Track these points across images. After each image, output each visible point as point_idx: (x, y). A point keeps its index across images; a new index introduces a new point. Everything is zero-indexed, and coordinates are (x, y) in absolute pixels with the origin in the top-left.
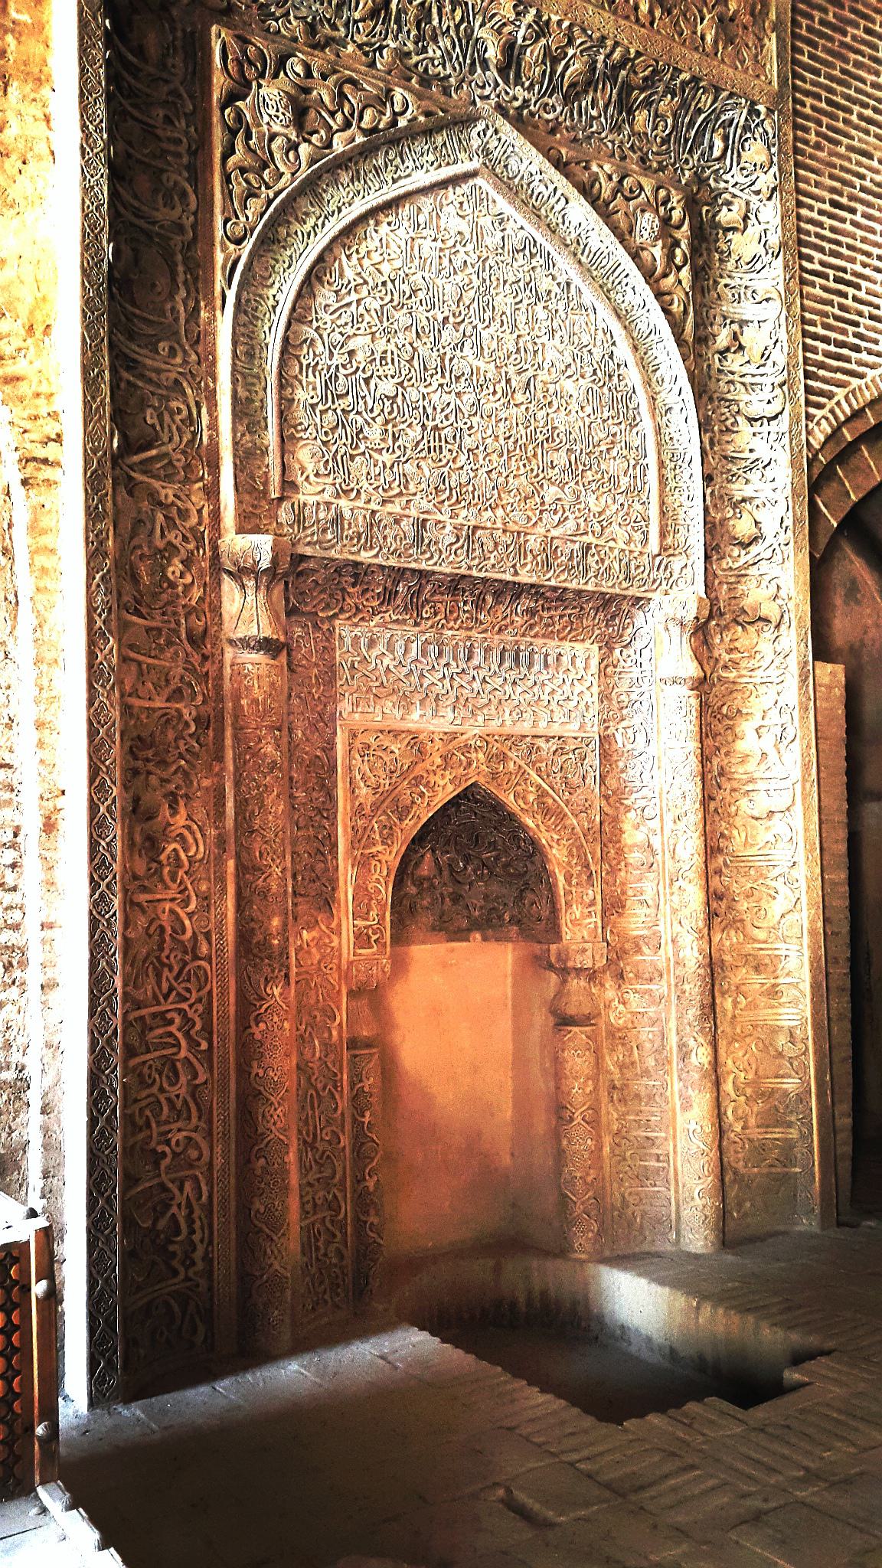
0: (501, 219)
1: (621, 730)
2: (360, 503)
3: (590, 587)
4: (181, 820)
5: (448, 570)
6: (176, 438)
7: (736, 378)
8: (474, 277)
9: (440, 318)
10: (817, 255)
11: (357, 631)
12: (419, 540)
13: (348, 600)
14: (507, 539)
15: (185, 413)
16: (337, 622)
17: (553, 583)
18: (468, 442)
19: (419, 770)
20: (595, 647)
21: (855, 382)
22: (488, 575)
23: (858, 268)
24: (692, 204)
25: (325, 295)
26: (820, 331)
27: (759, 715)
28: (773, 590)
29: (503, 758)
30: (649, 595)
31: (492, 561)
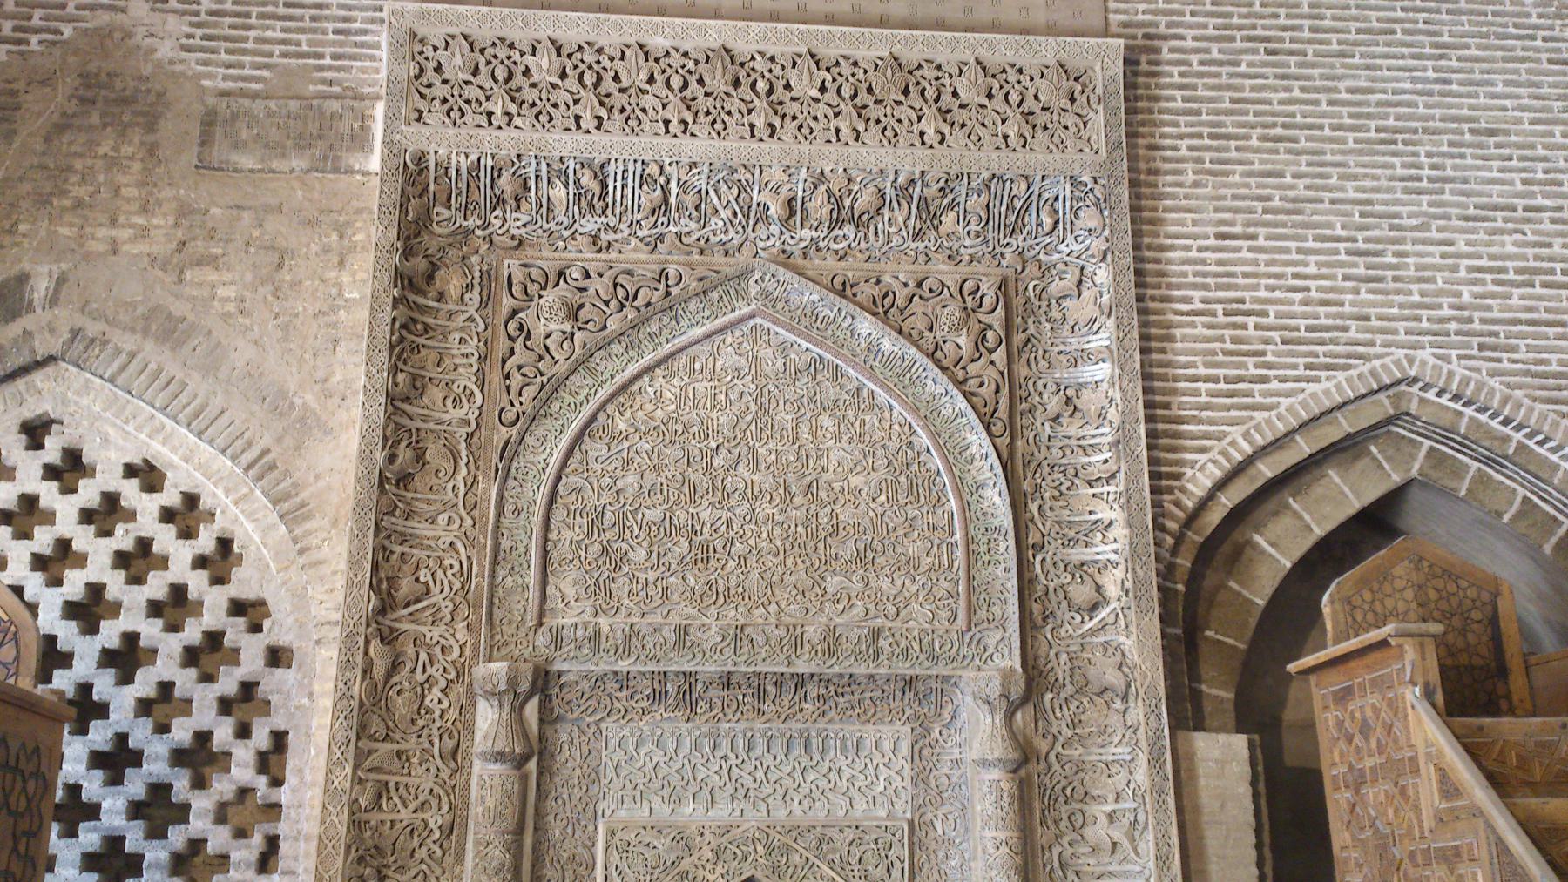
0: (784, 348)
1: (940, 816)
2: (620, 617)
3: (883, 671)
5: (713, 669)
6: (447, 589)
7: (1074, 442)
8: (752, 405)
9: (713, 445)
10: (1197, 294)
11: (626, 732)
12: (680, 644)
13: (616, 704)
14: (783, 633)
15: (457, 567)
16: (603, 726)
17: (837, 669)
19: (686, 864)
20: (907, 728)
22: (758, 669)
23: (1263, 294)
25: (595, 448)
26: (1202, 371)
27: (1111, 797)
28: (1118, 658)
30: (959, 673)
31: (764, 655)
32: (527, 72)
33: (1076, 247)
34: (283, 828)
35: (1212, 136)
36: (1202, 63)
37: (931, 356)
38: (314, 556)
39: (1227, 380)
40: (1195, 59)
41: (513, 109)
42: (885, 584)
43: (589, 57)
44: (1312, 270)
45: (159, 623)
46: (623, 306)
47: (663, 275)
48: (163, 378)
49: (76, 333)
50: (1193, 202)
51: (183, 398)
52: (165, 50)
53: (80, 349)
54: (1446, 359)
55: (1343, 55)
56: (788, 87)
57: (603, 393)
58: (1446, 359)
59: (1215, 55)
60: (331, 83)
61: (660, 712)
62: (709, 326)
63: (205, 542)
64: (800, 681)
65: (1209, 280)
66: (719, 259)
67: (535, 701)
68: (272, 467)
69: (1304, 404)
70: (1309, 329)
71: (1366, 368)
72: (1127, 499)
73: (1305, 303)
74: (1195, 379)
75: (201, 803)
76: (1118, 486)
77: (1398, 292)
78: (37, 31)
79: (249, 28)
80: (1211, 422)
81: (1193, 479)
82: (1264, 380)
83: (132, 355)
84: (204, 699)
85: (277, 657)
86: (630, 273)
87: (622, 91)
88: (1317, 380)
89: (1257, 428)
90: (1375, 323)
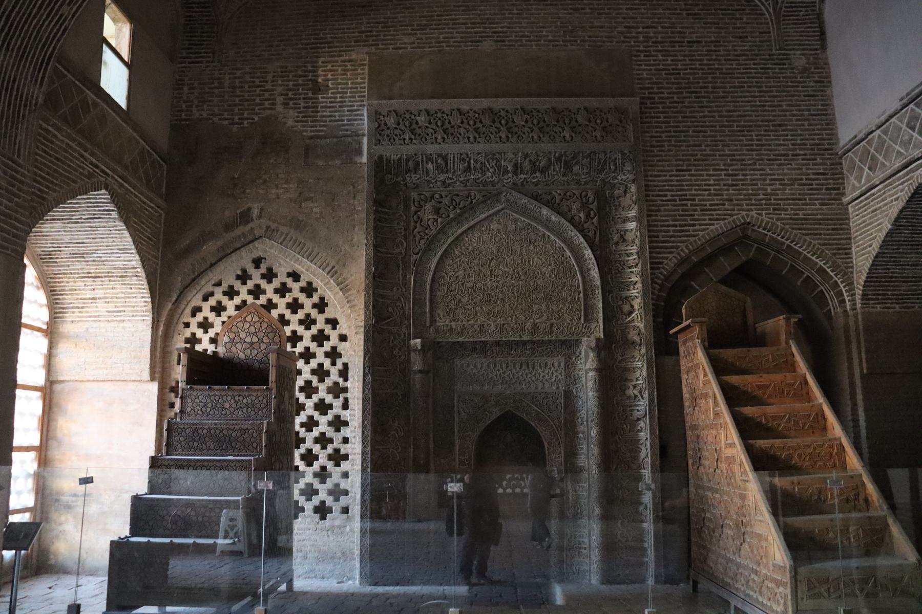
4: (396, 424)
12: (481, 331)
18: (501, 296)
21: (692, 239)
23: (694, 192)
24: (599, 194)
29: (521, 401)
32: (417, 123)
33: (624, 177)
34: (349, 395)
35: (675, 132)
36: (670, 103)
37: (570, 222)
38: (353, 303)
39: (680, 226)
40: (668, 101)
41: (413, 137)
42: (554, 307)
43: (439, 115)
44: (712, 182)
45: (303, 327)
46: (455, 208)
47: (469, 195)
48: (297, 243)
49: (268, 228)
50: (668, 158)
51: (305, 249)
52: (290, 123)
53: (270, 233)
54: (761, 215)
55: (724, 97)
56: (513, 122)
57: (449, 241)
58: (761, 215)
59: (675, 99)
60: (347, 130)
61: (475, 355)
62: (487, 214)
63: (315, 299)
64: (525, 343)
65: (674, 188)
66: (490, 187)
67: (430, 353)
68: (336, 272)
69: (708, 234)
70: (710, 205)
71: (731, 219)
72: (643, 274)
73: (709, 195)
74: (669, 226)
75: (322, 387)
76: (639, 268)
77: (744, 190)
78: (247, 119)
79: (318, 112)
80: (673, 242)
81: (667, 264)
82: (694, 225)
83: (287, 235)
84: (320, 352)
85: (343, 338)
86: (457, 195)
87: (452, 127)
88: (713, 224)
89: (691, 244)
90: (735, 202)
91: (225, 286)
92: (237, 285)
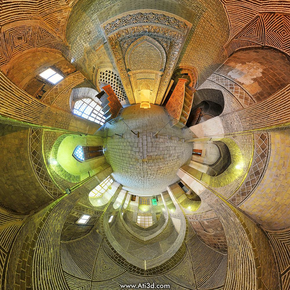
85: (118, 76)
91: (100, 80)
92: (101, 78)
